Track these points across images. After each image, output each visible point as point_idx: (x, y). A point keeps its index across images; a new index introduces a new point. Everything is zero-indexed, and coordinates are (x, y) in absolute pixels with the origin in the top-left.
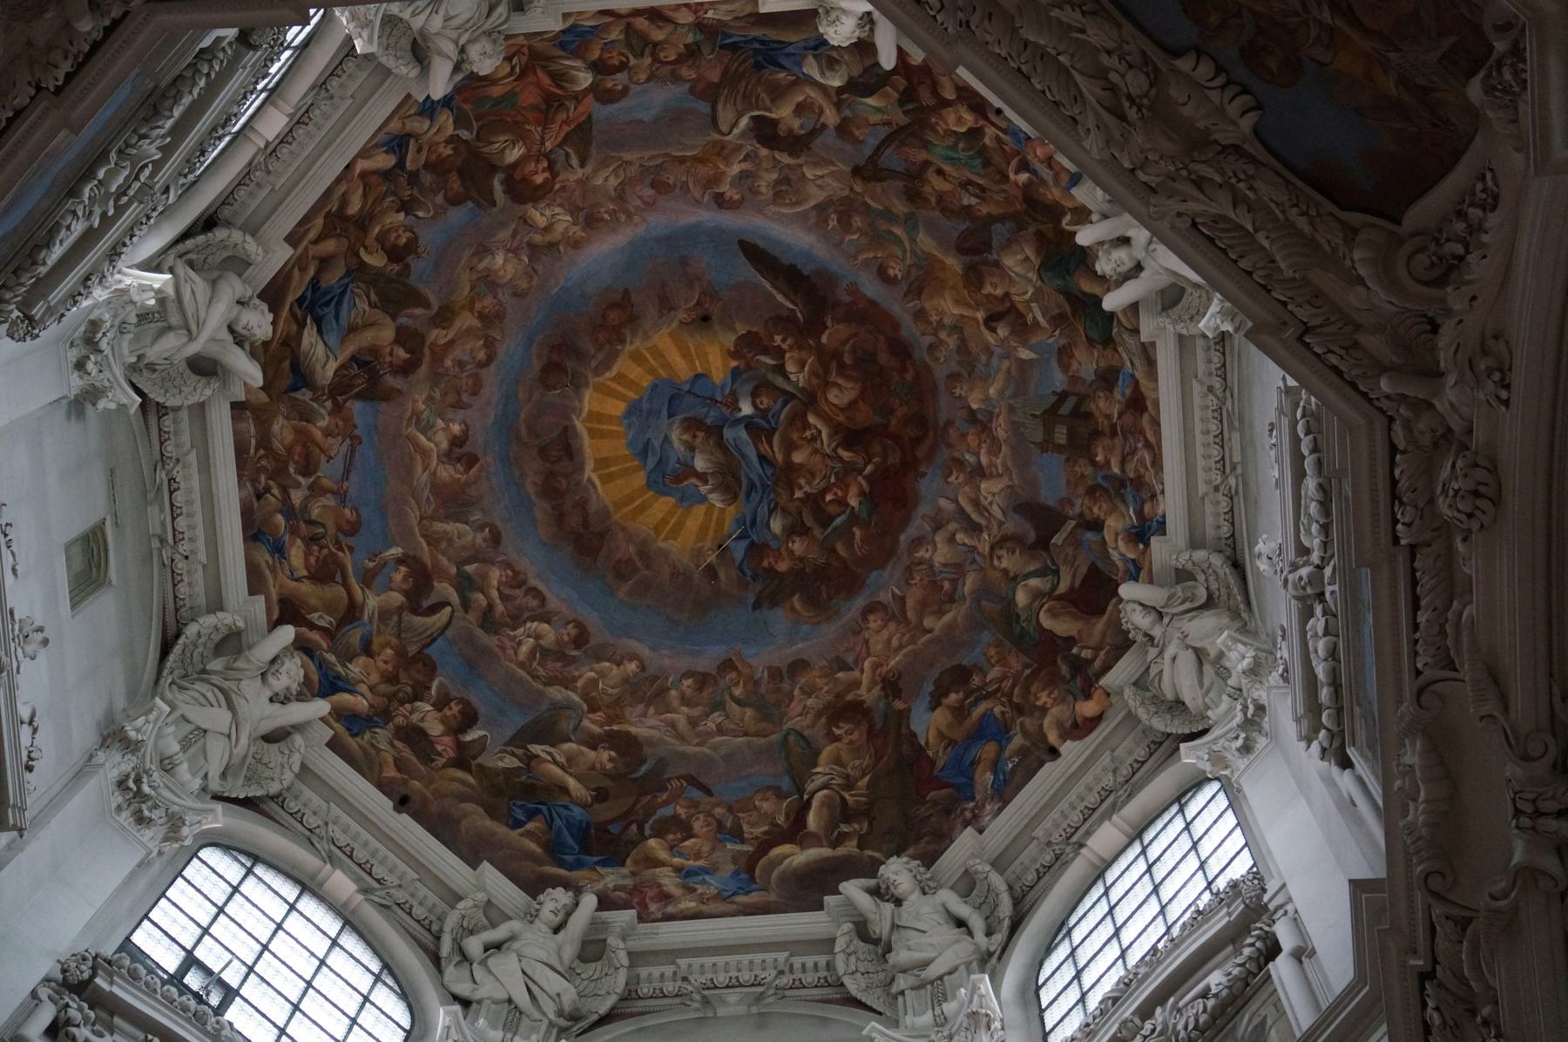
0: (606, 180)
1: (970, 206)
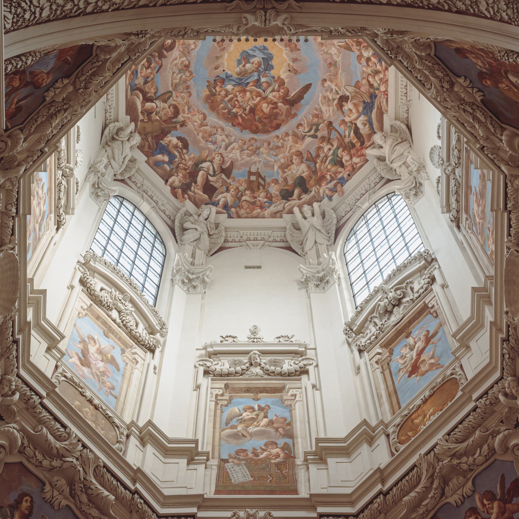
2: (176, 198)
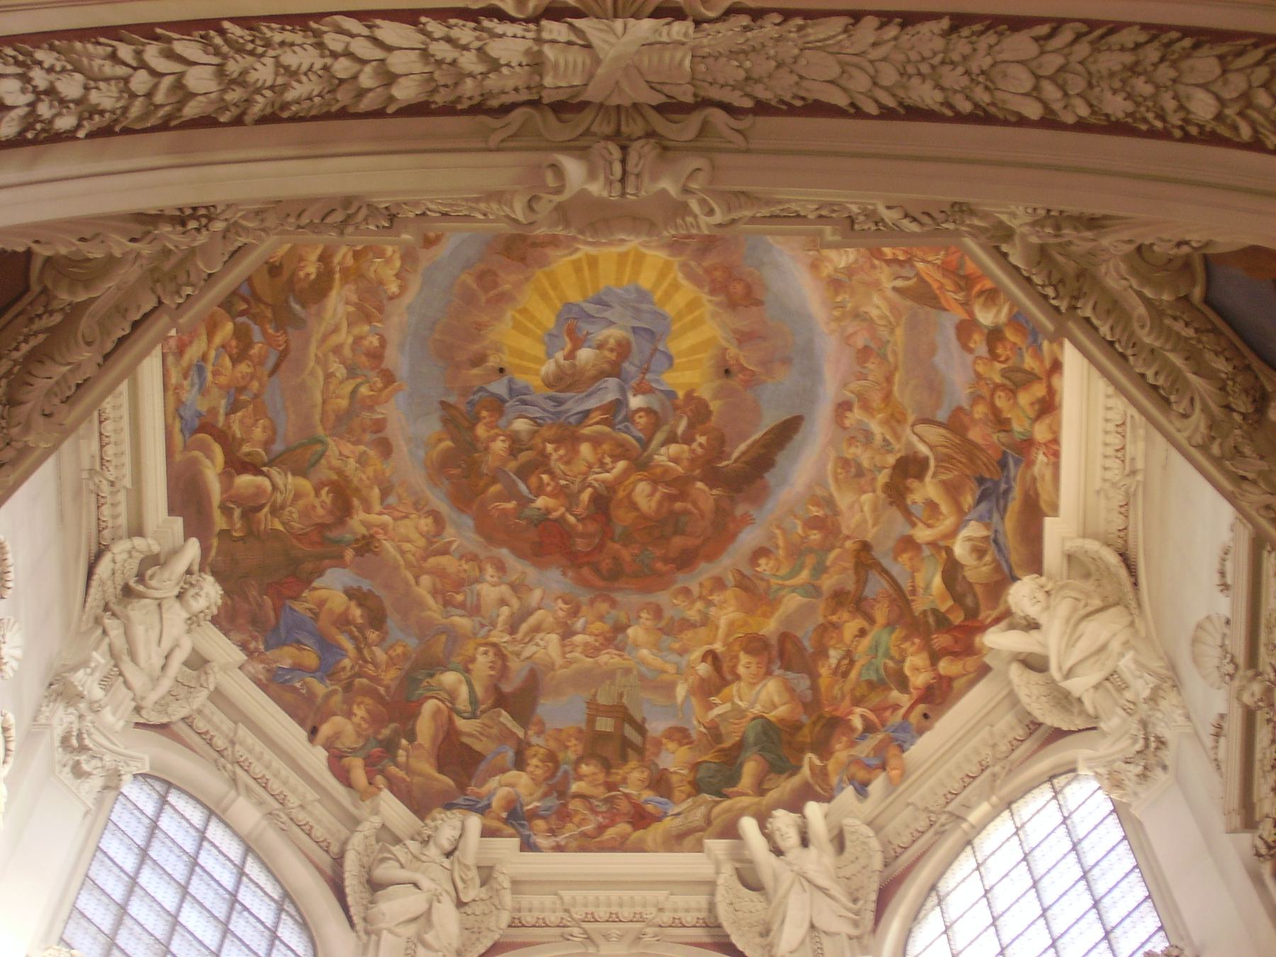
0: (877, 307)
1: (827, 657)
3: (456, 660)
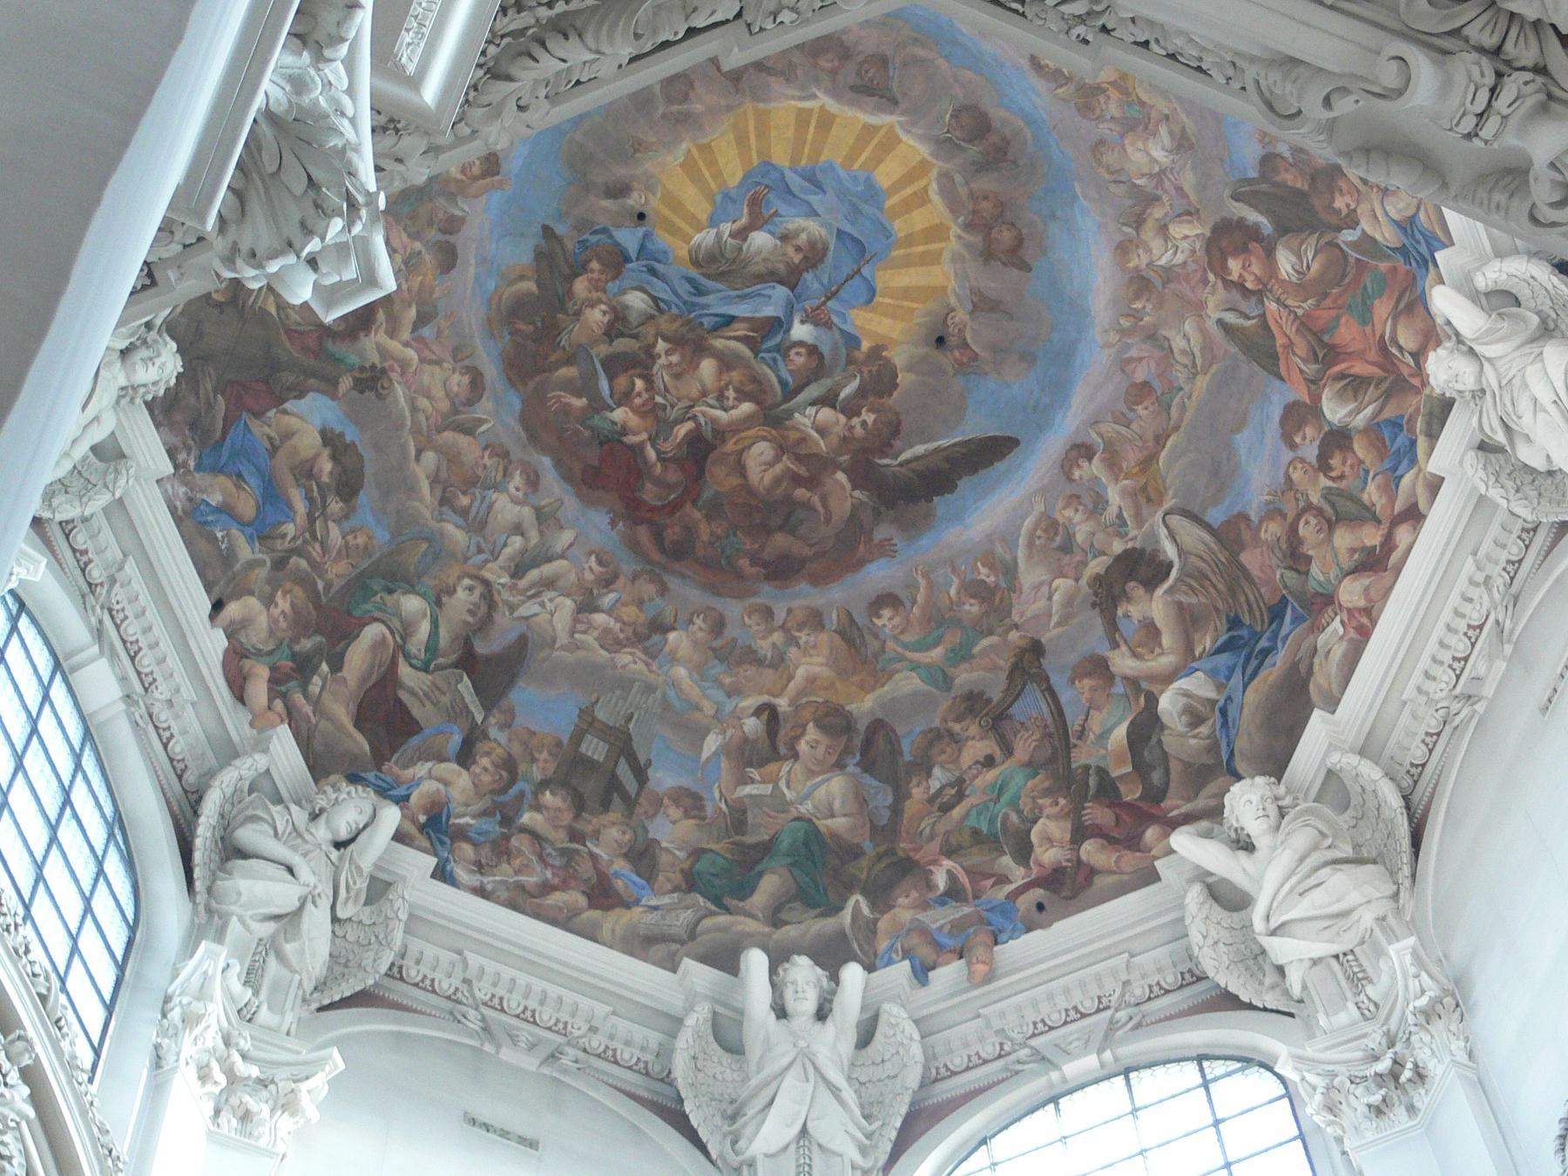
0: (1185, 336)
1: (929, 775)
2: (240, 695)
3: (428, 582)
